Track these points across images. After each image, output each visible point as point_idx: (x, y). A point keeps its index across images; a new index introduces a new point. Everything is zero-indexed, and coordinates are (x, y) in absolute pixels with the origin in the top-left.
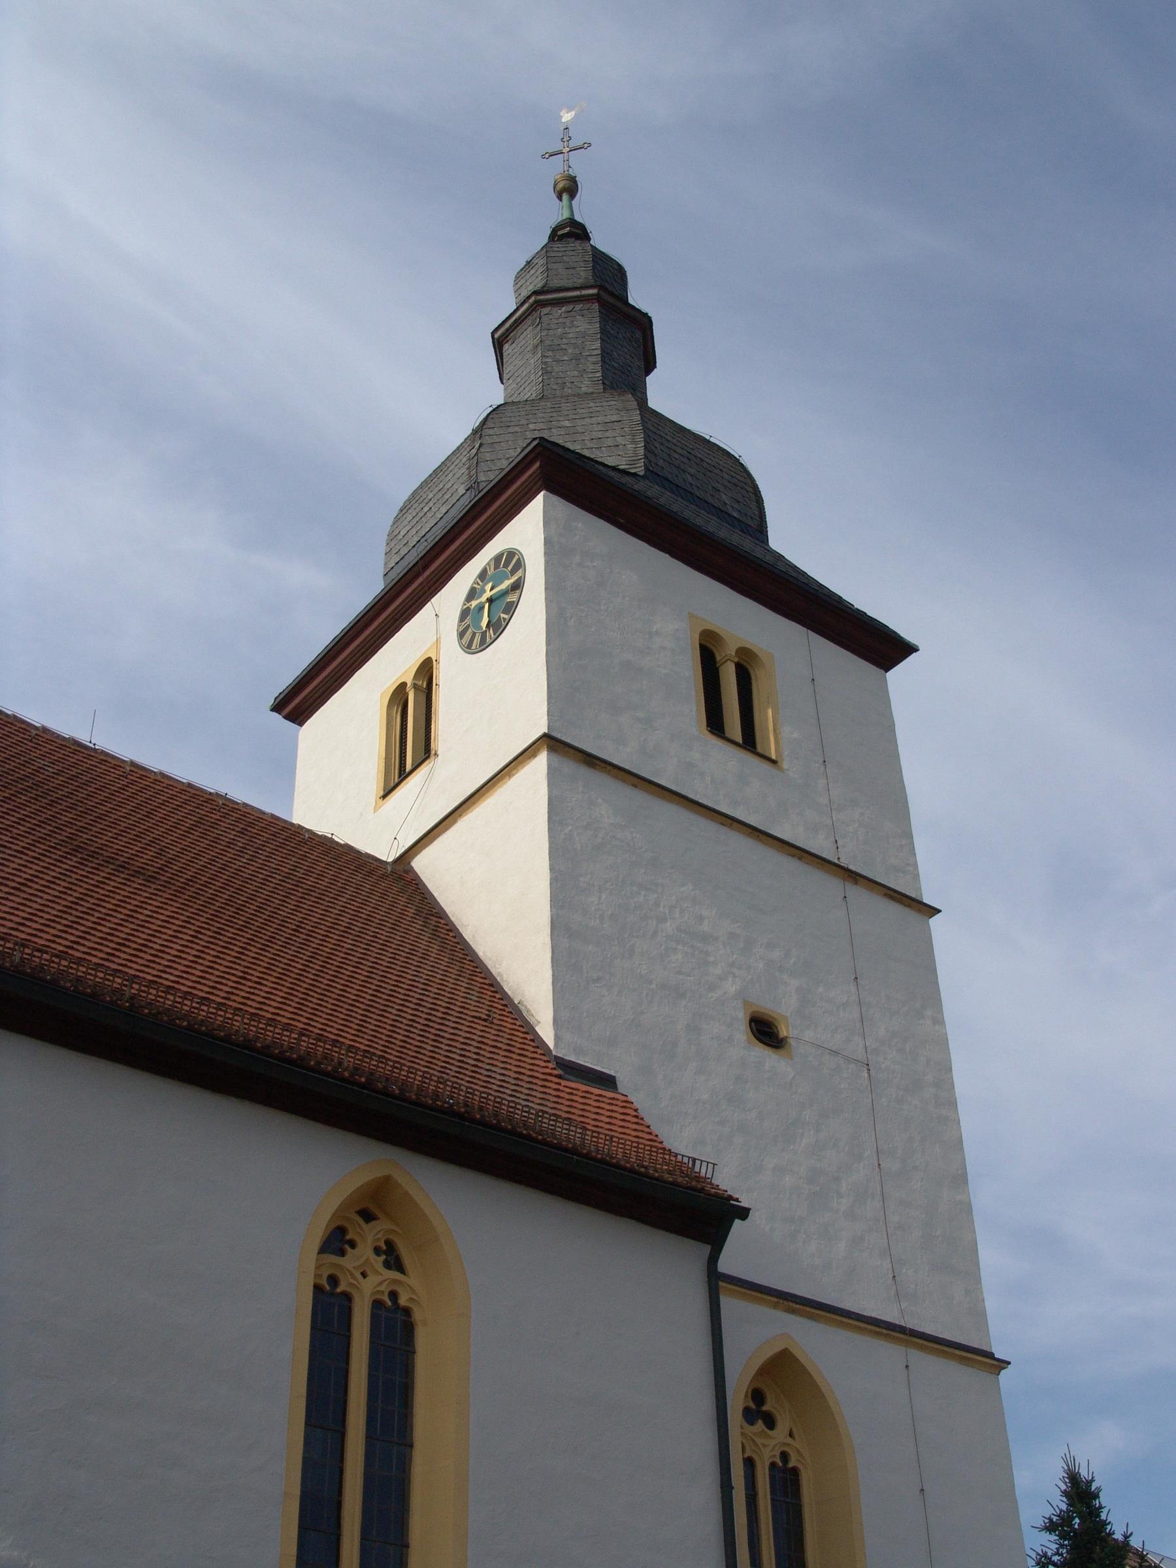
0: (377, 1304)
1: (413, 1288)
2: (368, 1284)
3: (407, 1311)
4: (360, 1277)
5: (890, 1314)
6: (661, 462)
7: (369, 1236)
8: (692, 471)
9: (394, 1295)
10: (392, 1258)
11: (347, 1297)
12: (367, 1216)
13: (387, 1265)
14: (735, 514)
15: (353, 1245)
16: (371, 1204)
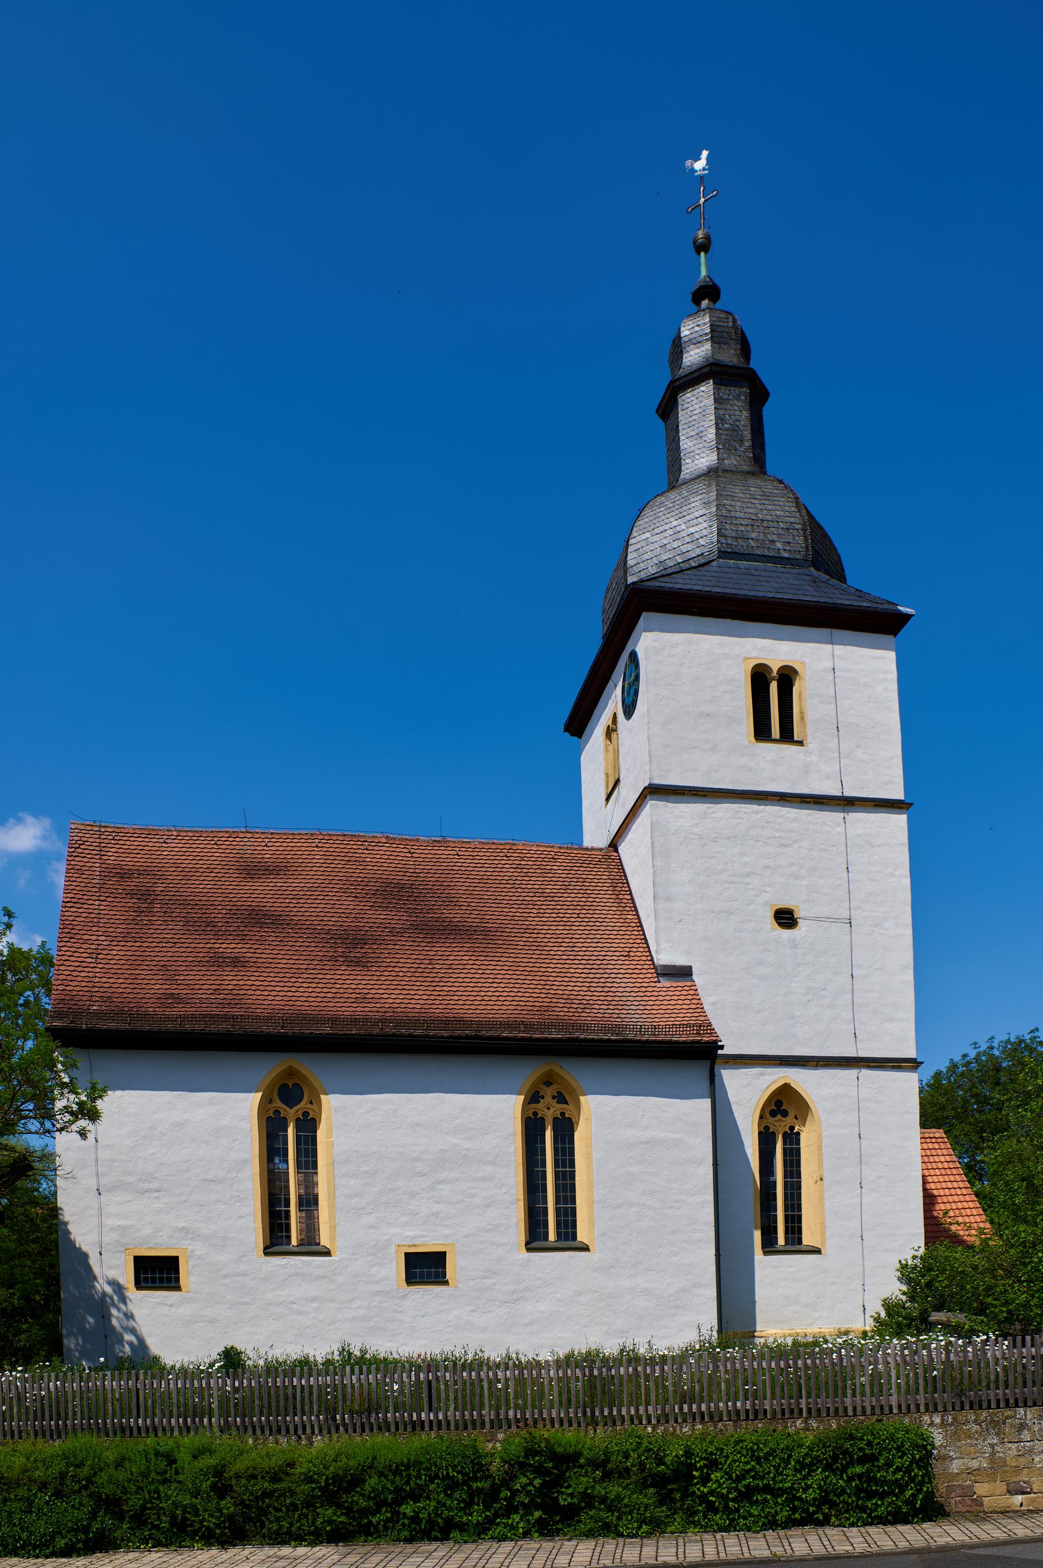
0: (555, 1119)
1: (569, 1110)
2: (549, 1110)
3: (570, 1119)
4: (546, 1110)
5: (848, 1051)
6: (730, 541)
7: (549, 1092)
8: (753, 535)
9: (563, 1114)
10: (561, 1099)
11: (542, 1119)
12: (548, 1084)
13: (558, 1102)
14: (786, 555)
15: (543, 1097)
16: (548, 1080)
